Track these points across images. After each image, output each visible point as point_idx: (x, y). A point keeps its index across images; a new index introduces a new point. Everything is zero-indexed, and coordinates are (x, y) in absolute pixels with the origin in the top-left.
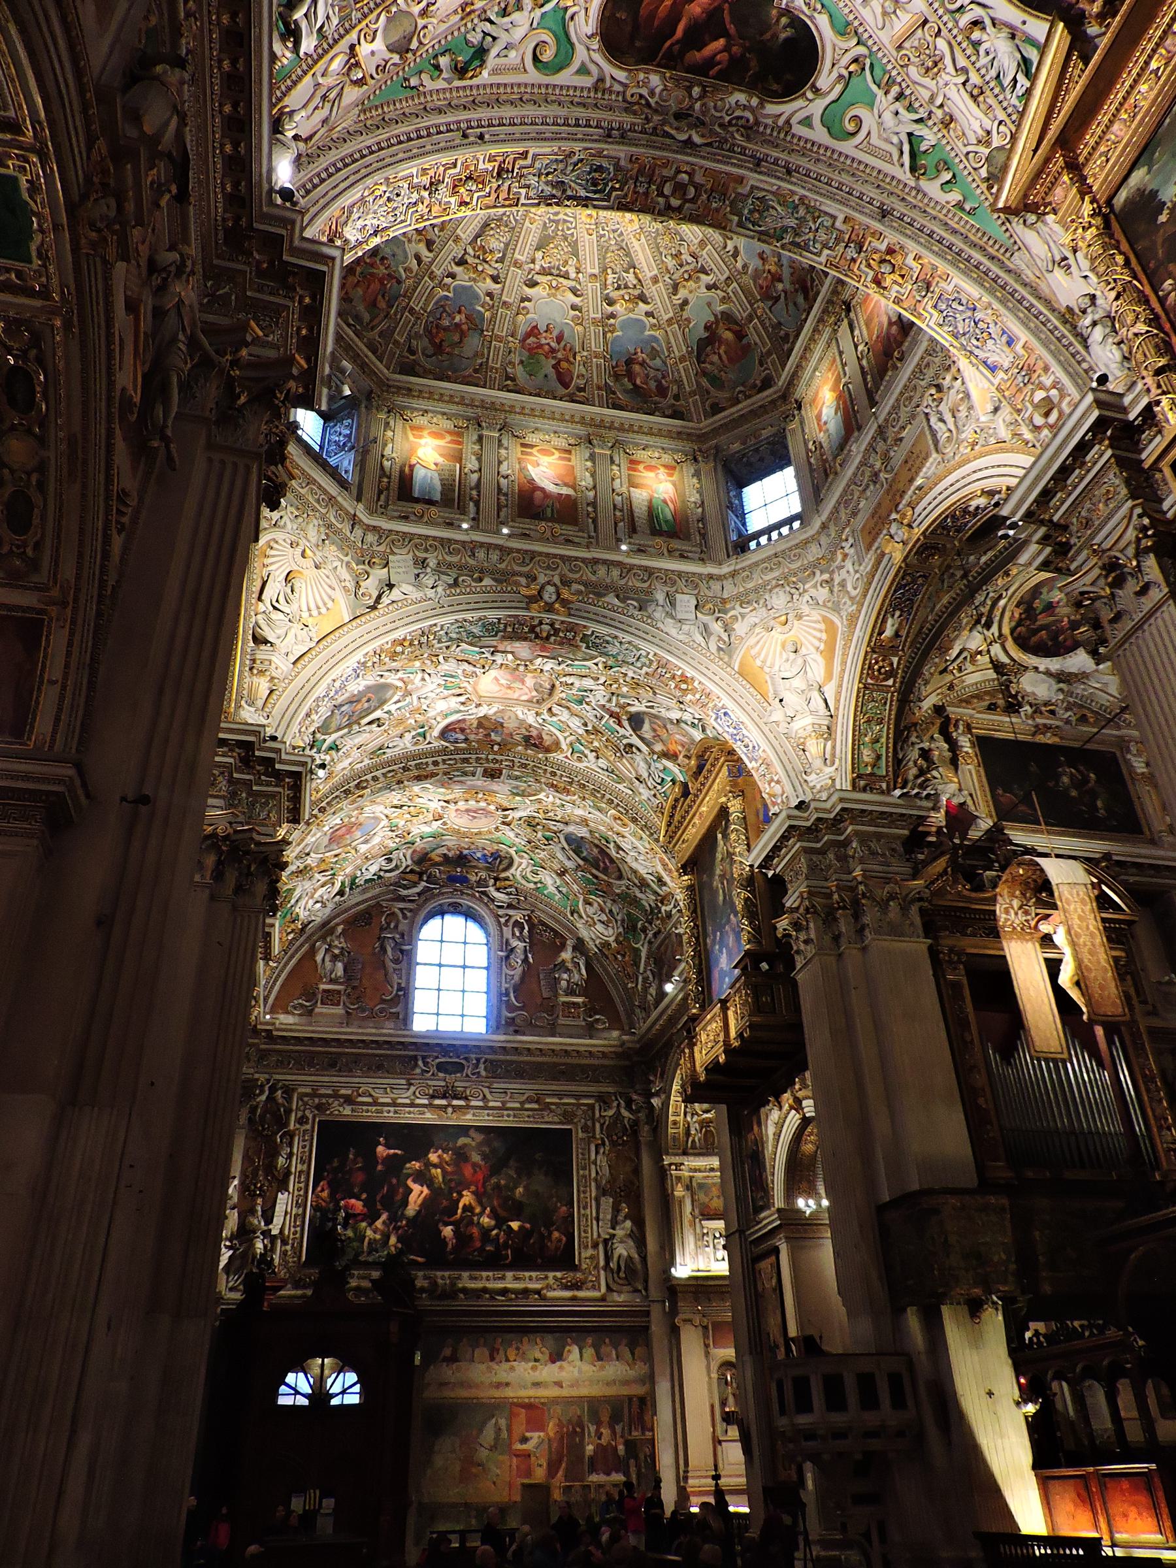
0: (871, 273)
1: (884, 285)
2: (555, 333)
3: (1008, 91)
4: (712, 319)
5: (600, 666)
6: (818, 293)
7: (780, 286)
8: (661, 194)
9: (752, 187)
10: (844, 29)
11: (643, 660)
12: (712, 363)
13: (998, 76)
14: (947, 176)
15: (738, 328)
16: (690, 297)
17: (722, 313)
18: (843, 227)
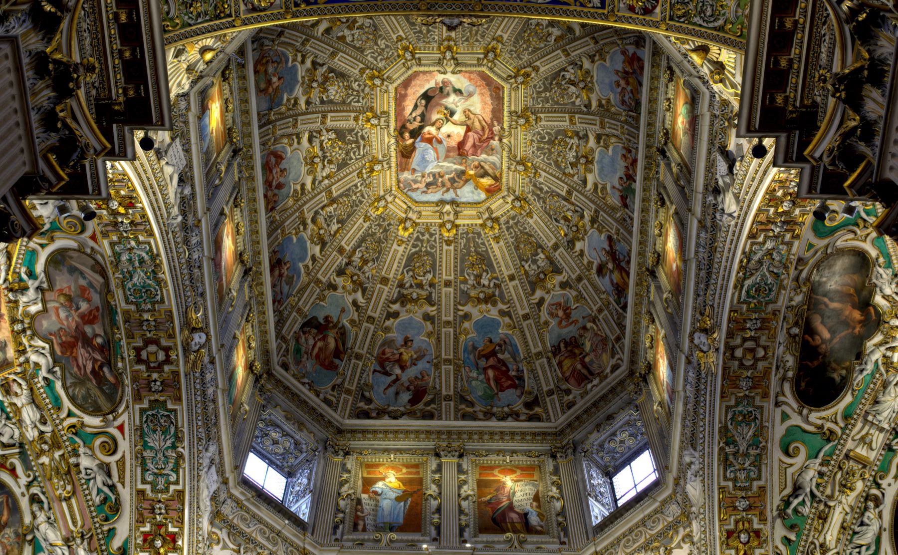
0: (732, 527)
1: (730, 541)
2: (282, 180)
3: (852, 545)
4: (335, 320)
5: (73, 420)
6: (431, 416)
7: (398, 371)
8: (745, 340)
9: (762, 407)
10: (847, 416)
11: (162, 481)
12: (306, 340)
13: (858, 533)
14: (793, 537)
15: (341, 349)
16: (340, 290)
17: (343, 327)
18: (755, 488)
